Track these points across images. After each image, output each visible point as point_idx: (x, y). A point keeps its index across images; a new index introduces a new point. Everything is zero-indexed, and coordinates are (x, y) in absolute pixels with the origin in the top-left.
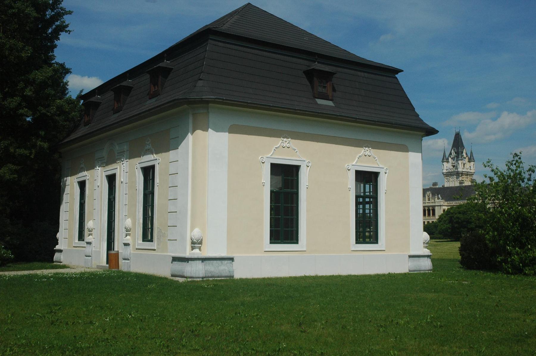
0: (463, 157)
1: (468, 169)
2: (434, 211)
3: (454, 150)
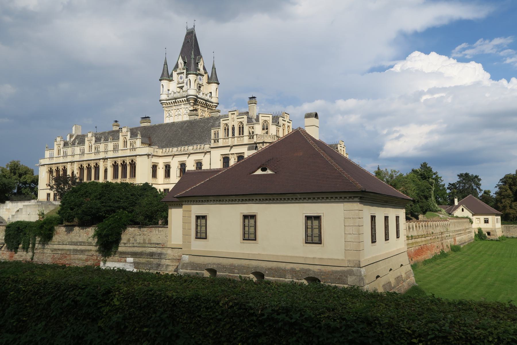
1: (206, 95)
2: (133, 165)
3: (183, 59)
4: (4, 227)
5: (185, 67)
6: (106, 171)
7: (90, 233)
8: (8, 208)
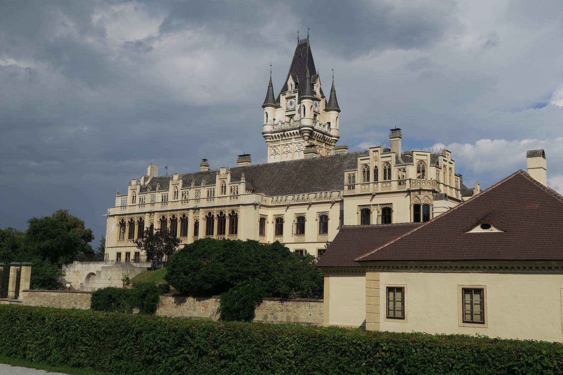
1: (324, 126)
2: (234, 218)
3: (294, 79)
4: (89, 294)
5: (296, 90)
6: (196, 225)
7: (209, 306)
8: (76, 270)
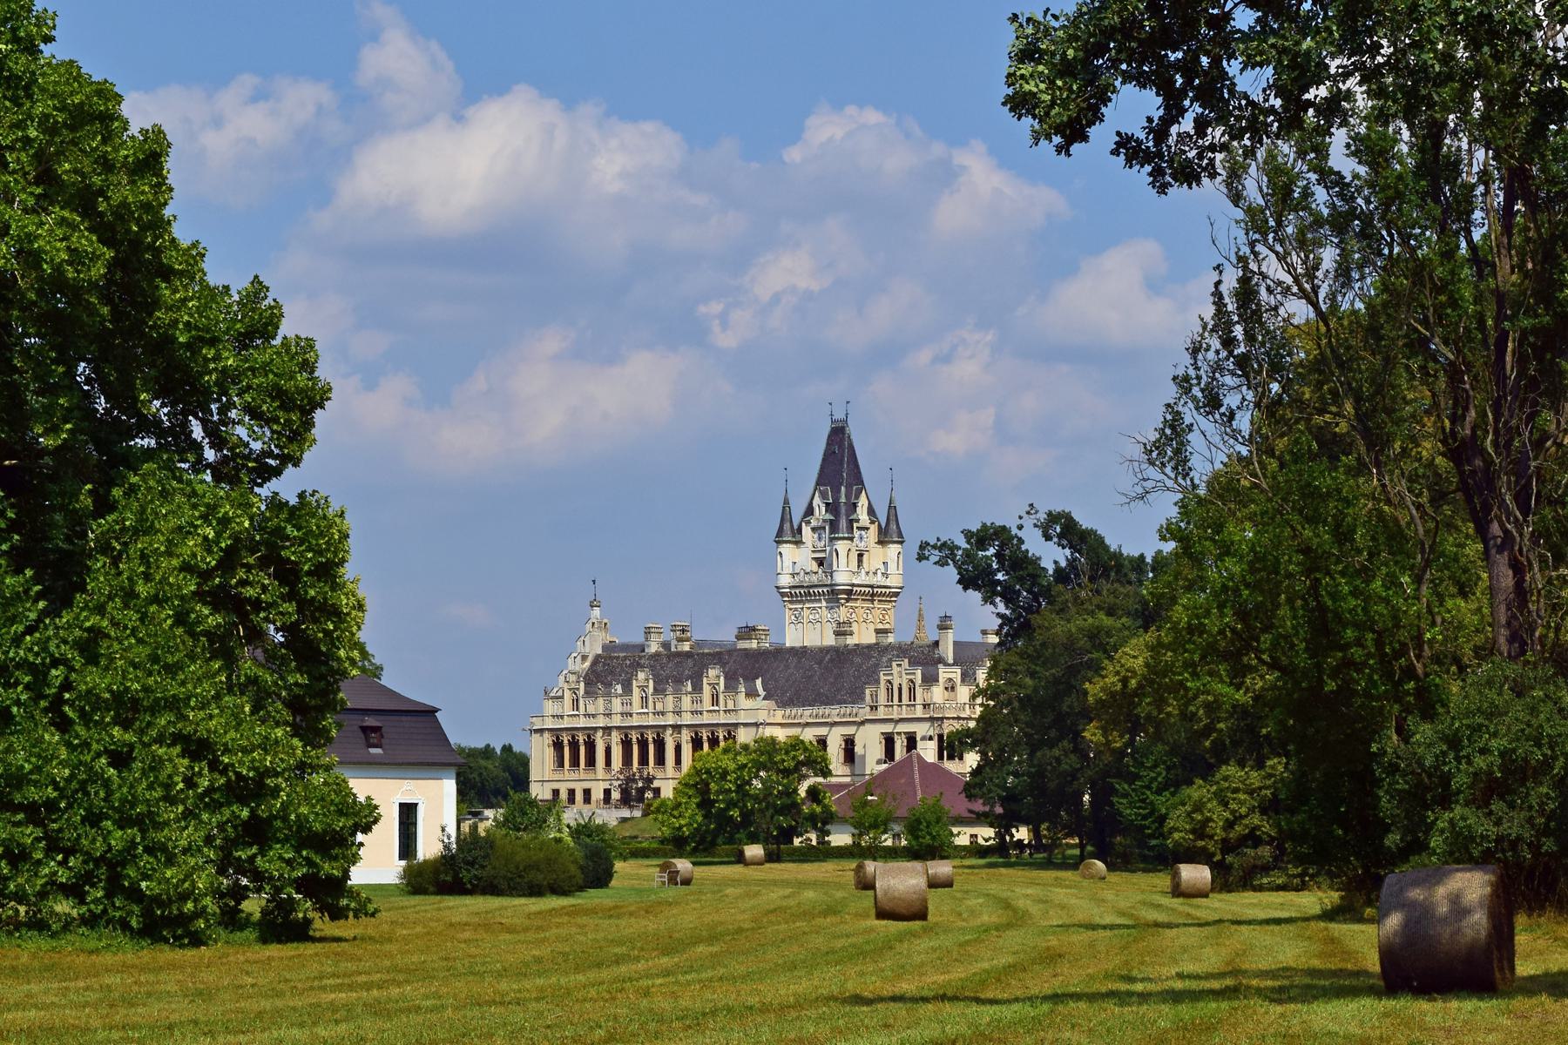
0: (855, 525)
1: (875, 573)
3: (824, 496)
6: (678, 749)
